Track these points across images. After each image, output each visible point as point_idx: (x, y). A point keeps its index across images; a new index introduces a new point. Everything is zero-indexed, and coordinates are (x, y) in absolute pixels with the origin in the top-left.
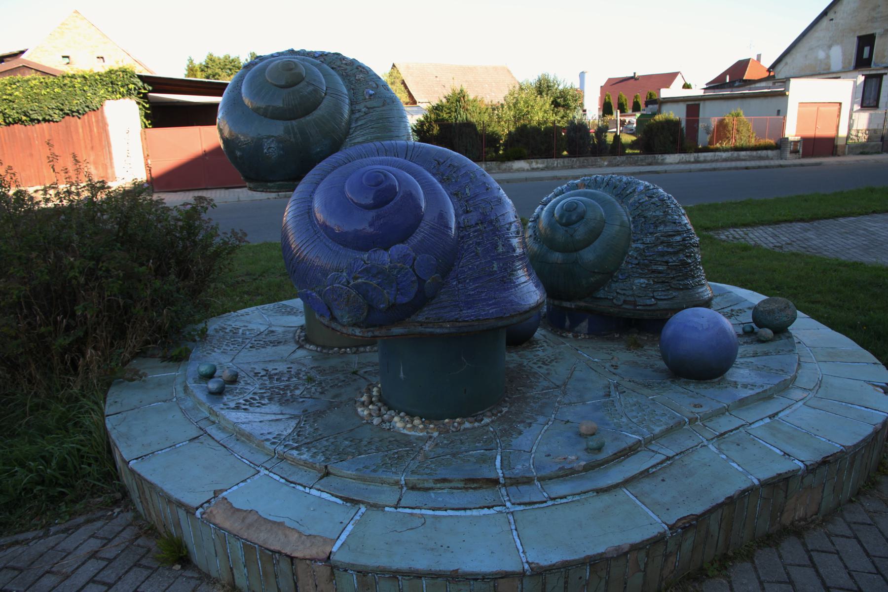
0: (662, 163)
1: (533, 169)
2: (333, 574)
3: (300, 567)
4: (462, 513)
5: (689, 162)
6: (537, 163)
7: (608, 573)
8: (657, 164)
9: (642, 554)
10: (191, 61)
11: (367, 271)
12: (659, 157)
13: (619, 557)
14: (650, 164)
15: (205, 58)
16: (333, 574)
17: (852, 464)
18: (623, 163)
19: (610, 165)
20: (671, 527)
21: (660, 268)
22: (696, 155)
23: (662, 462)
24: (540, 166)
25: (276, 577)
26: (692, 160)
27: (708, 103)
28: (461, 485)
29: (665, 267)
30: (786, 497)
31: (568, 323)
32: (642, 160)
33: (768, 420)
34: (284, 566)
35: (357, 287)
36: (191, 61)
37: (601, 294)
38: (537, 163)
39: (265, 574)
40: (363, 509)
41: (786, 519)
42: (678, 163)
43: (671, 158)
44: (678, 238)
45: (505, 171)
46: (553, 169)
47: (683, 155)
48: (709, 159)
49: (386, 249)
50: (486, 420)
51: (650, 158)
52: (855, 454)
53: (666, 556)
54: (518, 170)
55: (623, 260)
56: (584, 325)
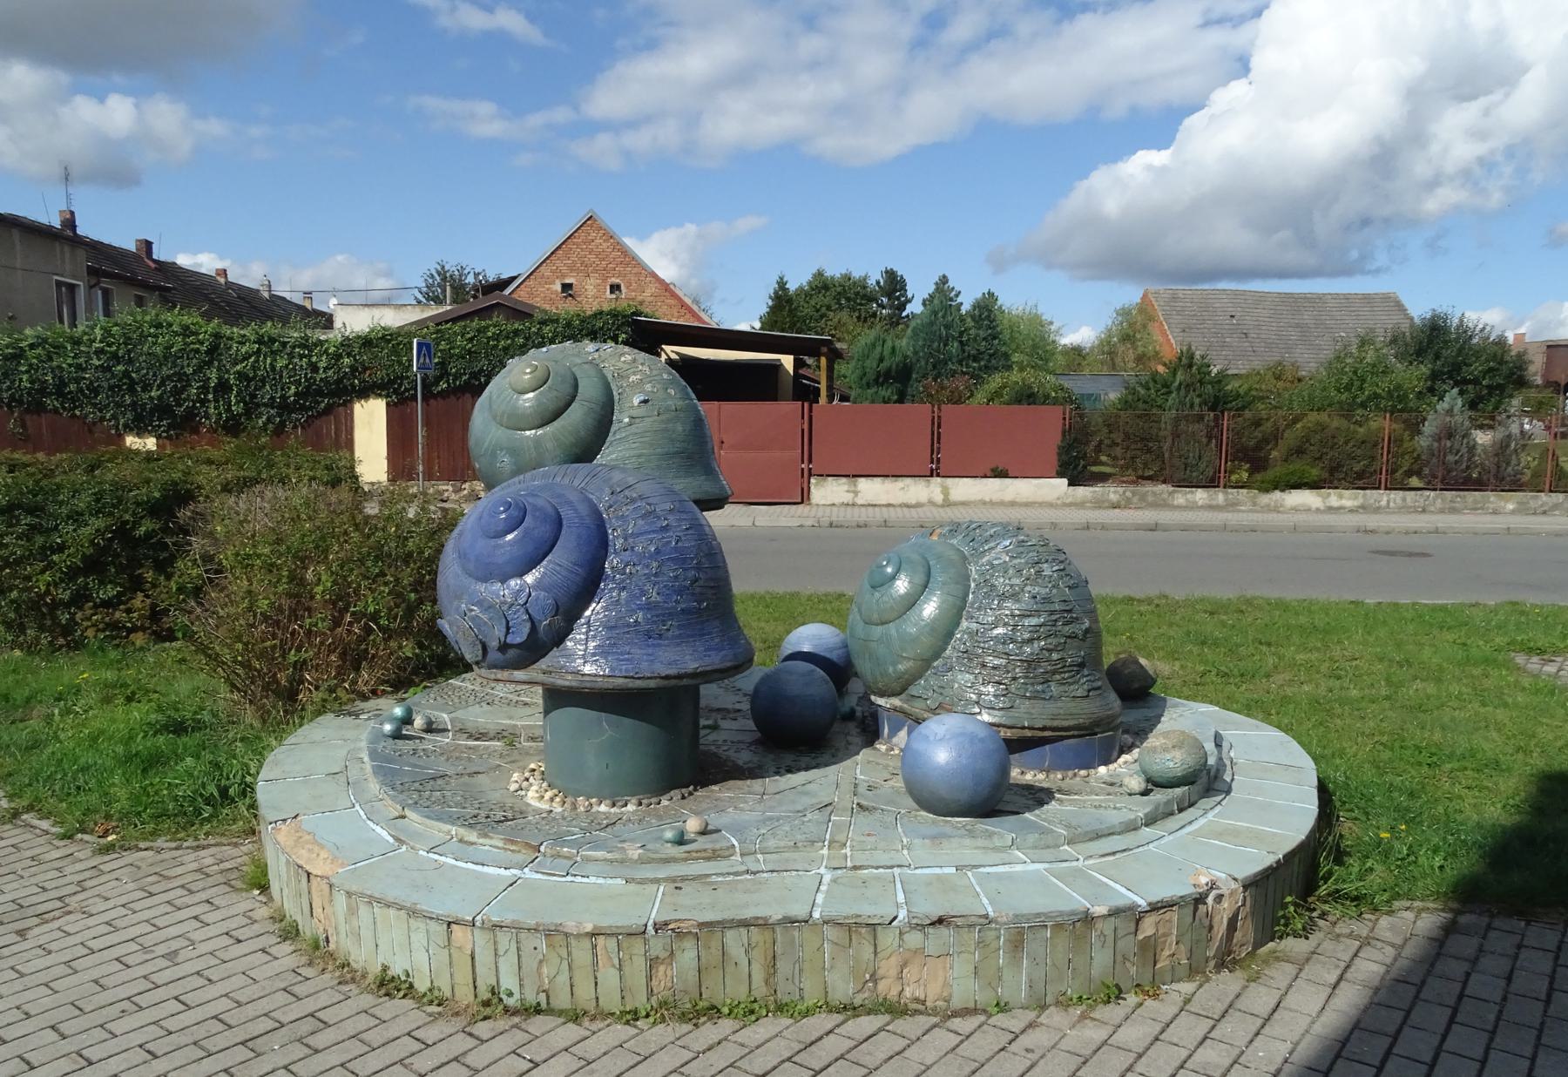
1: (1330, 509)
3: (314, 881)
4: (479, 868)
6: (1341, 497)
7: (569, 954)
10: (782, 284)
13: (579, 936)
15: (810, 277)
18: (1556, 506)
19: (1522, 510)
23: (736, 874)
24: (1348, 503)
28: (500, 844)
29: (1004, 662)
30: (876, 953)
33: (953, 870)
36: (782, 284)
37: (913, 690)
38: (1341, 497)
41: (888, 988)
44: (1034, 621)
45: (1269, 509)
46: (1377, 510)
49: (503, 581)
50: (631, 808)
52: (1021, 932)
53: (653, 963)
54: (1295, 509)
55: (947, 643)
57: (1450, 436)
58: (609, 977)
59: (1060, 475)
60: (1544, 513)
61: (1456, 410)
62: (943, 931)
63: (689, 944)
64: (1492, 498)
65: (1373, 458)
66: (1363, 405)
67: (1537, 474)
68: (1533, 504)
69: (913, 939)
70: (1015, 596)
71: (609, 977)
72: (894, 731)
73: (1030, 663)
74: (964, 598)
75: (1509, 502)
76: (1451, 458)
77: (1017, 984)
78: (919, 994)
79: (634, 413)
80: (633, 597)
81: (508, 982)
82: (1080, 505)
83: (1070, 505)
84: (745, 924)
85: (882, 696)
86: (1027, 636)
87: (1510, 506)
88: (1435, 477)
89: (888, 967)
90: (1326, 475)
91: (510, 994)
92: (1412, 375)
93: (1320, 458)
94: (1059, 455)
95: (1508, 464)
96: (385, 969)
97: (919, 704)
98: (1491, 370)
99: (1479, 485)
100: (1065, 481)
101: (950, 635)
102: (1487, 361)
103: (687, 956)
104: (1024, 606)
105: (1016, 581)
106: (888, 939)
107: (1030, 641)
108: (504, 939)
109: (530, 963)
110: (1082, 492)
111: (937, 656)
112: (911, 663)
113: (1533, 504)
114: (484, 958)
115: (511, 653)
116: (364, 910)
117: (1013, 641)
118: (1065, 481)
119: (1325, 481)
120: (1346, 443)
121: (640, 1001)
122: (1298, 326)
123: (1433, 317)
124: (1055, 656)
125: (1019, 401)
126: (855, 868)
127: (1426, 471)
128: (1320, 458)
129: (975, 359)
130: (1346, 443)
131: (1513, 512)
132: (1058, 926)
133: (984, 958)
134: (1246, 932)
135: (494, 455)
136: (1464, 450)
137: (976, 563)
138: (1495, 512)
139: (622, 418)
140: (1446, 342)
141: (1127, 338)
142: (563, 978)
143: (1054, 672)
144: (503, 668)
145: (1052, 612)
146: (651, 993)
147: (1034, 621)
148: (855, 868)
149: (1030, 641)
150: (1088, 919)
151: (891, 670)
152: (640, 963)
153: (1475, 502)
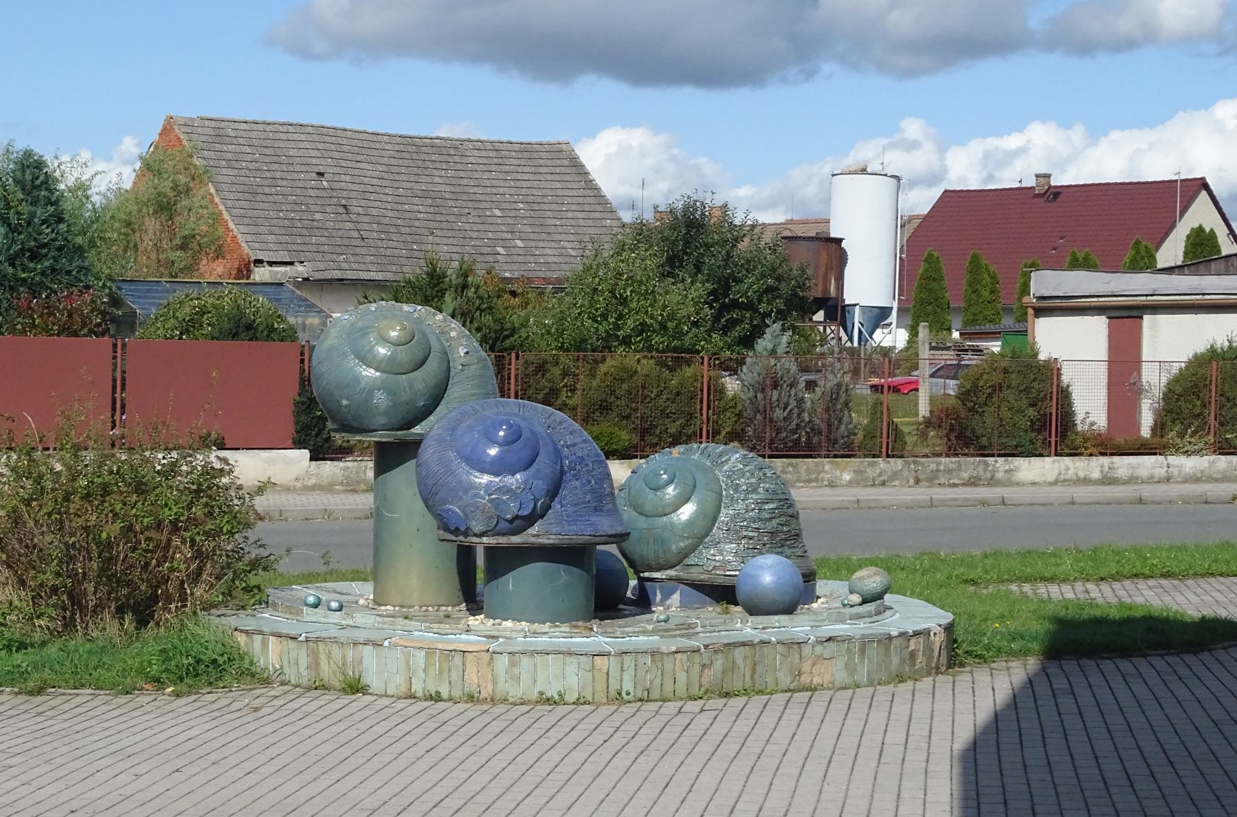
0: (1008, 483)
2: (492, 658)
5: (1086, 481)
8: (992, 482)
9: (684, 657)
11: (499, 489)
12: (1000, 465)
14: (973, 482)
16: (492, 658)
17: (863, 651)
18: (895, 475)
19: (860, 480)
20: (706, 647)
21: (751, 534)
22: (1105, 460)
25: (450, 670)
26: (1096, 475)
27: (1162, 318)
28: (567, 630)
31: (659, 597)
32: (949, 471)
34: (458, 659)
35: (491, 501)
37: (692, 560)
39: (441, 672)
40: (501, 640)
41: (805, 679)
42: (1055, 483)
43: (1037, 471)
44: (771, 506)
47: (1067, 460)
48: (1143, 473)
49: (513, 475)
51: (970, 465)
53: (704, 666)
56: (676, 597)
57: (775, 385)
58: (682, 677)
59: (298, 444)
60: (883, 484)
61: (780, 350)
62: (831, 644)
63: (719, 656)
64: (828, 467)
65: (691, 416)
66: (626, 341)
67: (870, 435)
68: (871, 473)
69: (819, 649)
70: (755, 490)
71: (682, 677)
72: (667, 595)
73: (772, 534)
74: (721, 494)
75: (844, 471)
76: (779, 414)
77: (863, 674)
78: (820, 681)
79: (462, 361)
80: (583, 485)
81: (628, 686)
82: (327, 488)
83: (313, 488)
84: (744, 644)
85: (658, 570)
86: (767, 516)
87: (847, 477)
88: (760, 439)
89: (806, 667)
90: (636, 439)
91: (628, 694)
92: (685, 297)
93: (628, 417)
94: (297, 414)
95: (840, 421)
96: (541, 693)
97: (693, 570)
98: (769, 289)
99: (809, 451)
100: (306, 453)
101: (715, 519)
102: (763, 276)
103: (719, 663)
104: (762, 496)
105: (753, 480)
106: (807, 650)
107: (771, 519)
108: (628, 660)
109: (641, 673)
110: (329, 469)
111: (706, 535)
112: (690, 541)
113: (871, 473)
114: (614, 673)
115: (517, 522)
116: (526, 662)
117: (760, 520)
118: (306, 453)
119: (635, 447)
120: (659, 394)
121: (695, 691)
122: (425, 195)
123: (686, 208)
124: (785, 529)
125: (234, 335)
126: (764, 628)
127: (750, 431)
128: (628, 417)
129: (34, 257)
130: (659, 394)
131: (850, 484)
132: (879, 641)
133: (849, 658)
134: (944, 660)
135: (371, 393)
136: (793, 404)
137: (720, 471)
138: (831, 485)
139: (456, 367)
140: (708, 246)
141: (165, 208)
142: (658, 681)
143: (786, 540)
144: (504, 534)
145: (780, 500)
146: (701, 686)
147: (771, 506)
148: (764, 628)
149: (771, 519)
150: (890, 638)
151: (674, 547)
152: (697, 668)
153: (808, 470)
